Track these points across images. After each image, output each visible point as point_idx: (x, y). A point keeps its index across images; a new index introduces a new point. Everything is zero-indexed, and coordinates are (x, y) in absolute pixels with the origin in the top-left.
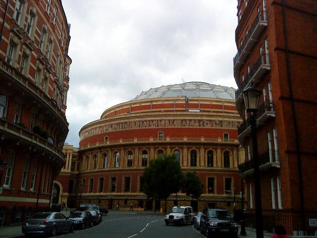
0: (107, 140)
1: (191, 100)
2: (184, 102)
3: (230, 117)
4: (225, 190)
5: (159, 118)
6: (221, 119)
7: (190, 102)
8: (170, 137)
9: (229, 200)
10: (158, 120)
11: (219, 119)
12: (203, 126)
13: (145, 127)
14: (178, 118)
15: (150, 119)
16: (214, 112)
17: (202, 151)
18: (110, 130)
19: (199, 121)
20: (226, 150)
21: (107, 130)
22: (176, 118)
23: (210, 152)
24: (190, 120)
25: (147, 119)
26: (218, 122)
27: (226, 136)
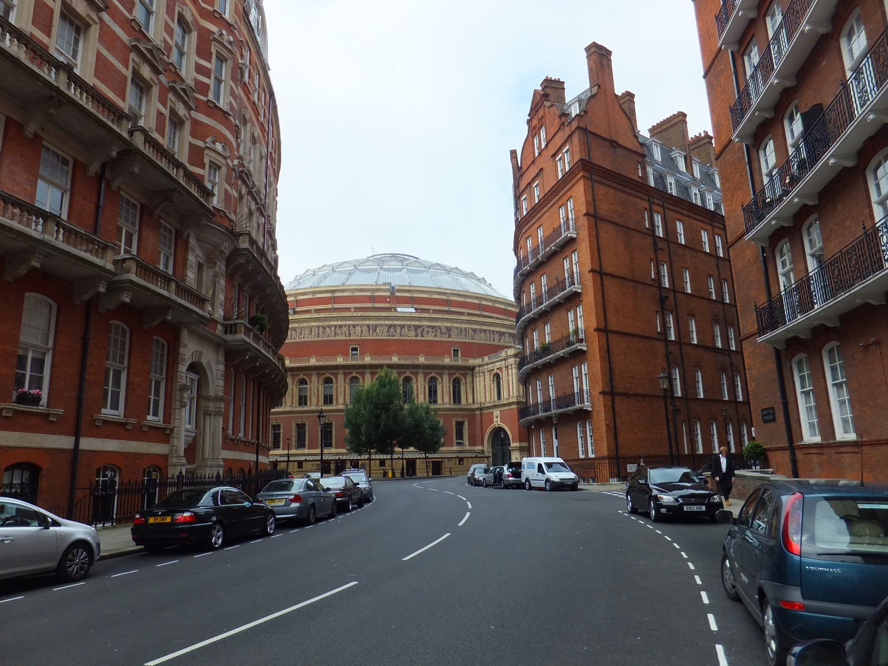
3: (462, 322)
4: (455, 441)
5: (352, 323)
6: (449, 325)
8: (371, 355)
9: (460, 455)
10: (349, 326)
11: (446, 324)
12: (422, 336)
14: (382, 322)
15: (336, 323)
17: (421, 377)
20: (454, 377)
22: (379, 322)
23: (433, 380)
24: (402, 327)
25: (332, 323)
26: (444, 330)
27: (456, 351)
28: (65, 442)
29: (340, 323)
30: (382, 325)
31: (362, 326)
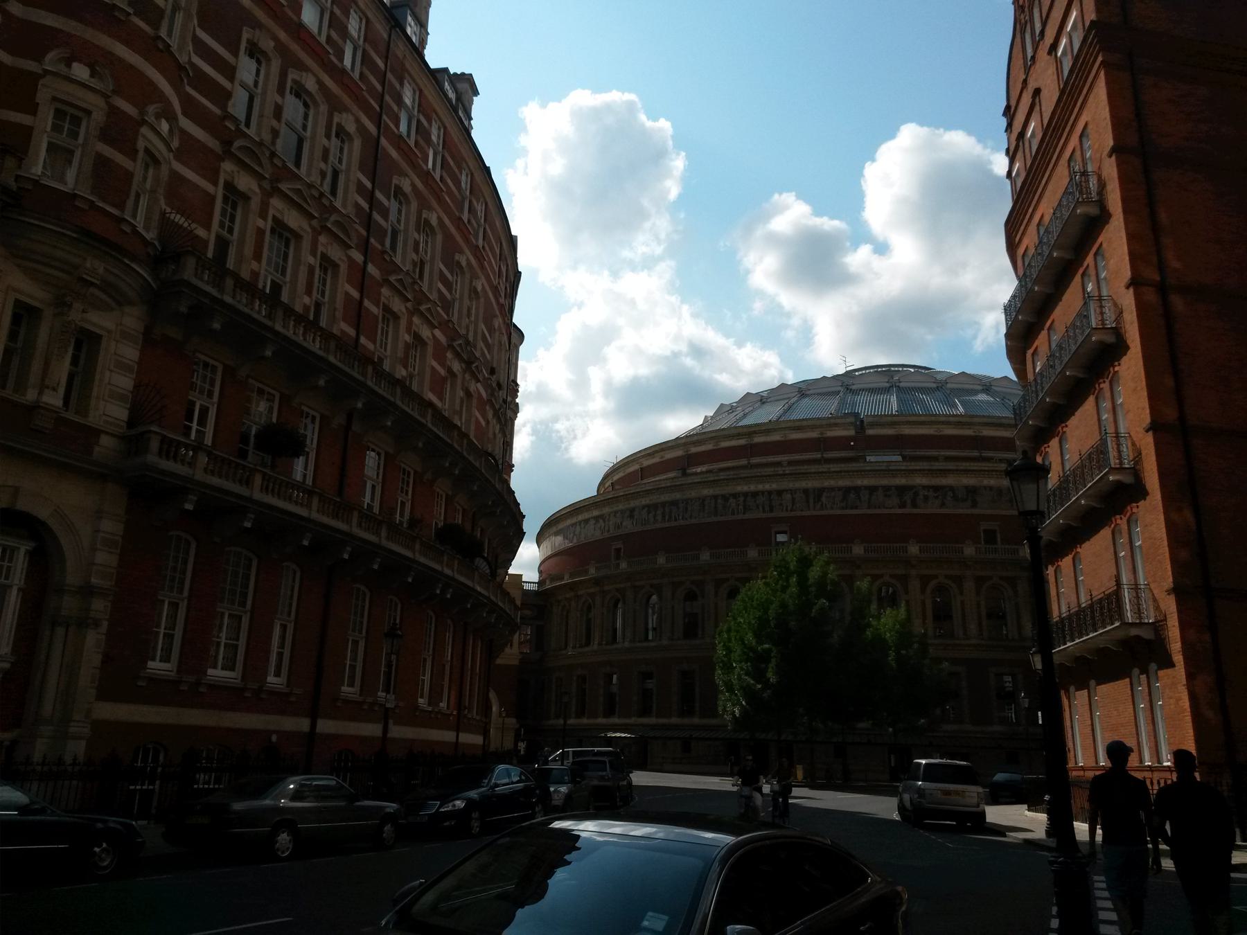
0: (618, 557)
1: (873, 425)
2: (852, 432)
5: (774, 486)
7: (870, 432)
10: (770, 493)
13: (733, 514)
14: (832, 483)
15: (746, 488)
16: (948, 459)
18: (629, 526)
19: (902, 490)
21: (618, 527)
22: (826, 484)
24: (872, 489)
25: (739, 489)
28: (304, 724)
29: (753, 488)
30: (832, 489)
31: (792, 491)
